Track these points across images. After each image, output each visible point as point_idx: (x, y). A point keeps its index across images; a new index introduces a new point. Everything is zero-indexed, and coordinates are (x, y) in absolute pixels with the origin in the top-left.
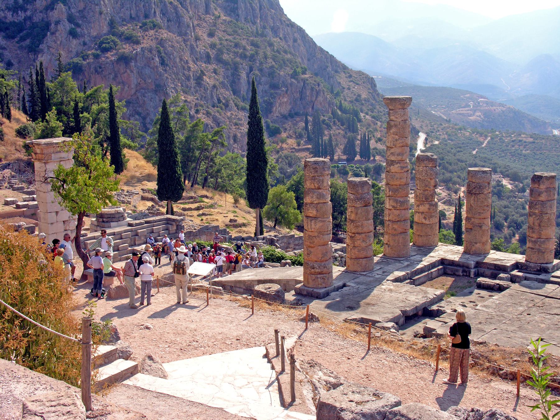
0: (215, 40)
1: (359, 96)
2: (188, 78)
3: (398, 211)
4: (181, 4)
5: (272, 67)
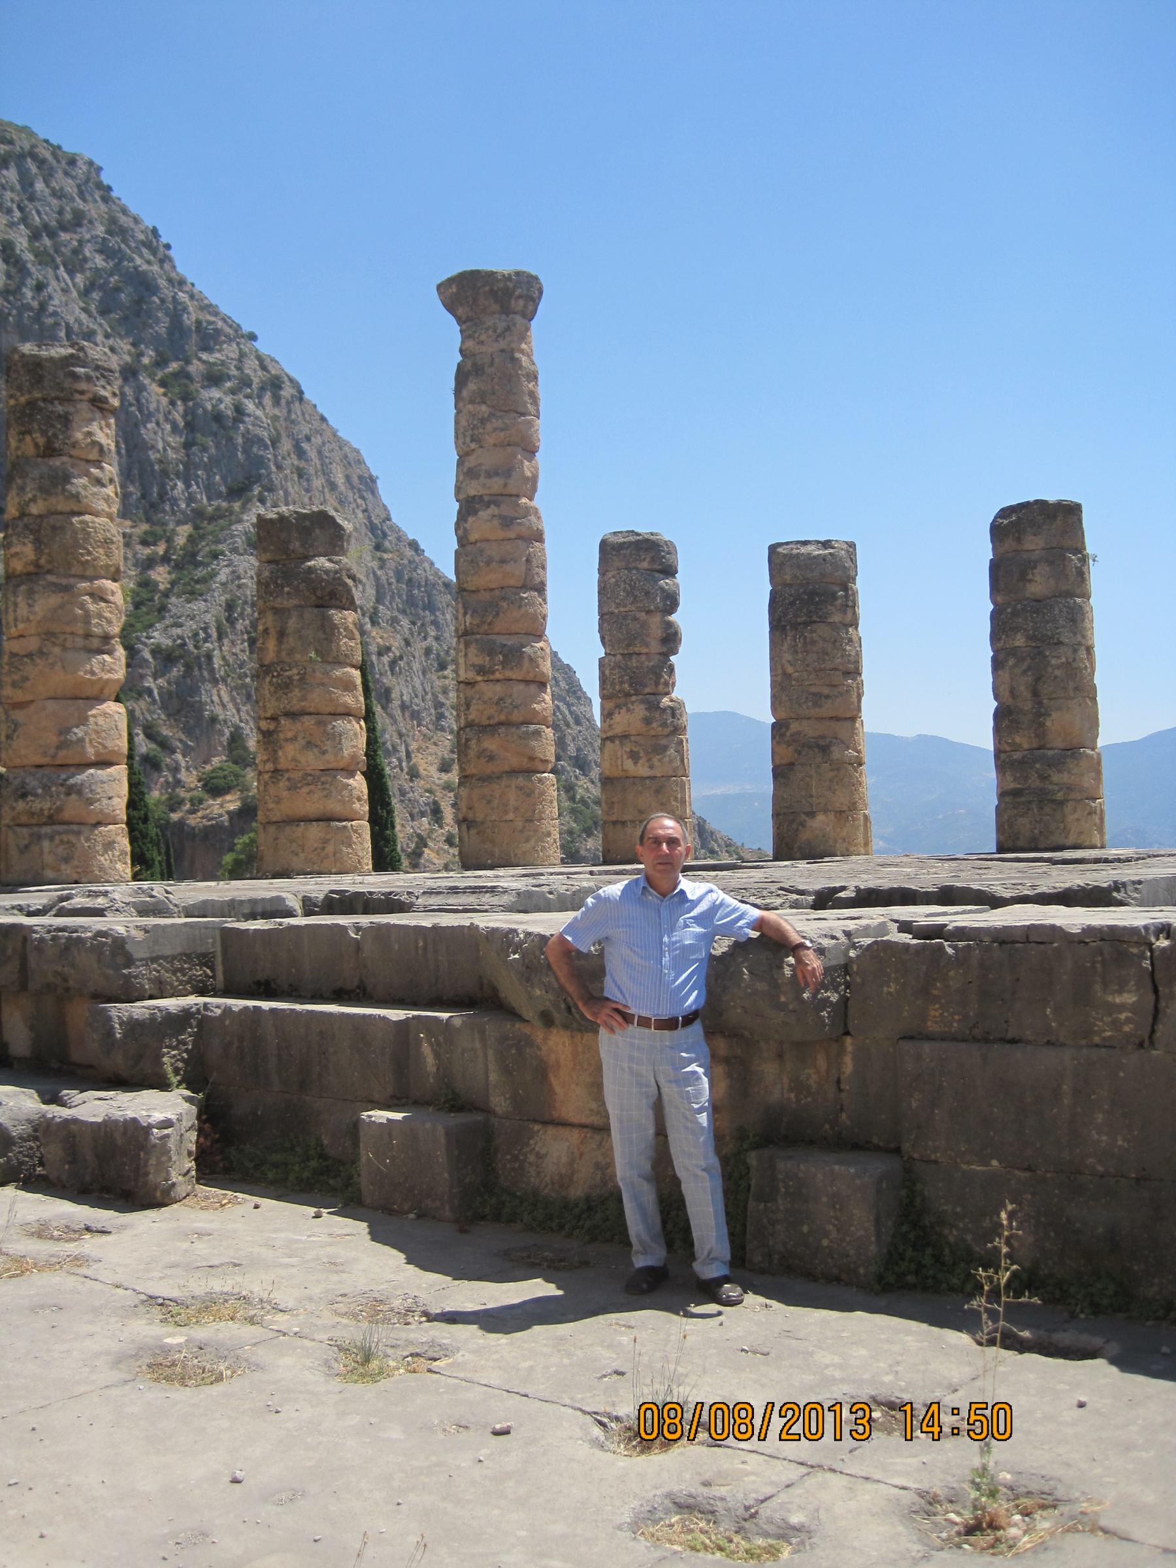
3: (498, 688)
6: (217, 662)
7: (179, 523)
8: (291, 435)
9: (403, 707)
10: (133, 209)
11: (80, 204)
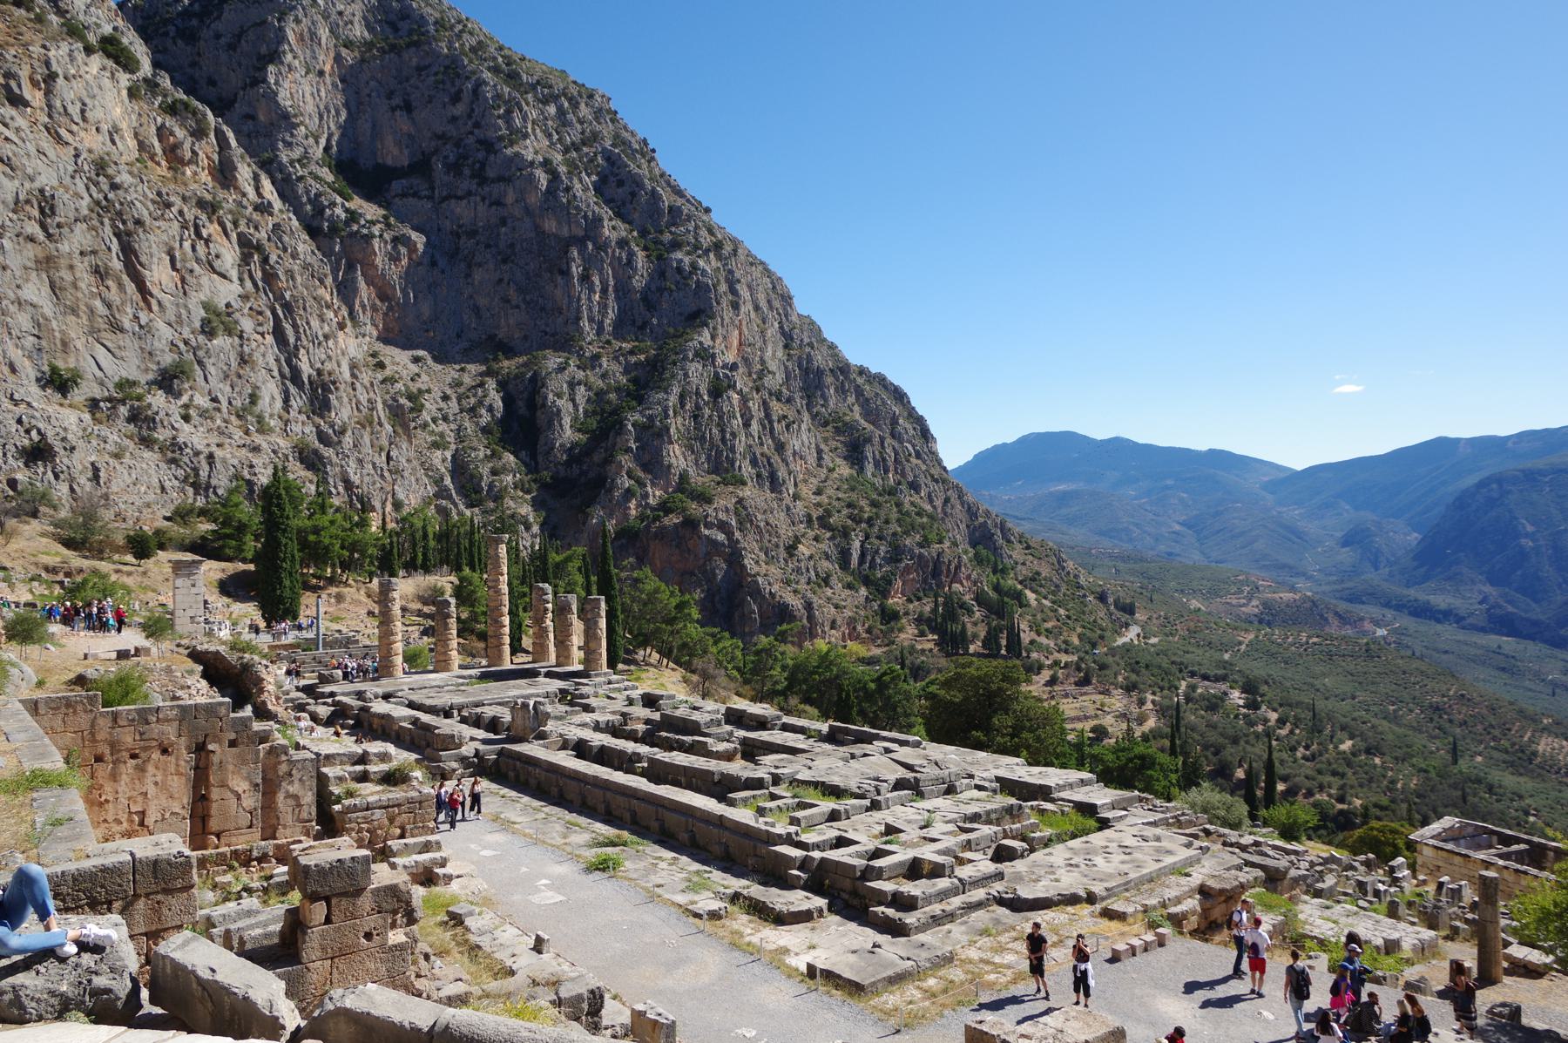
0: (824, 499)
1: (1038, 573)
2: (777, 546)
5: (894, 534)
6: (672, 431)
8: (727, 280)
9: (795, 453)
10: (631, 127)
11: (598, 128)
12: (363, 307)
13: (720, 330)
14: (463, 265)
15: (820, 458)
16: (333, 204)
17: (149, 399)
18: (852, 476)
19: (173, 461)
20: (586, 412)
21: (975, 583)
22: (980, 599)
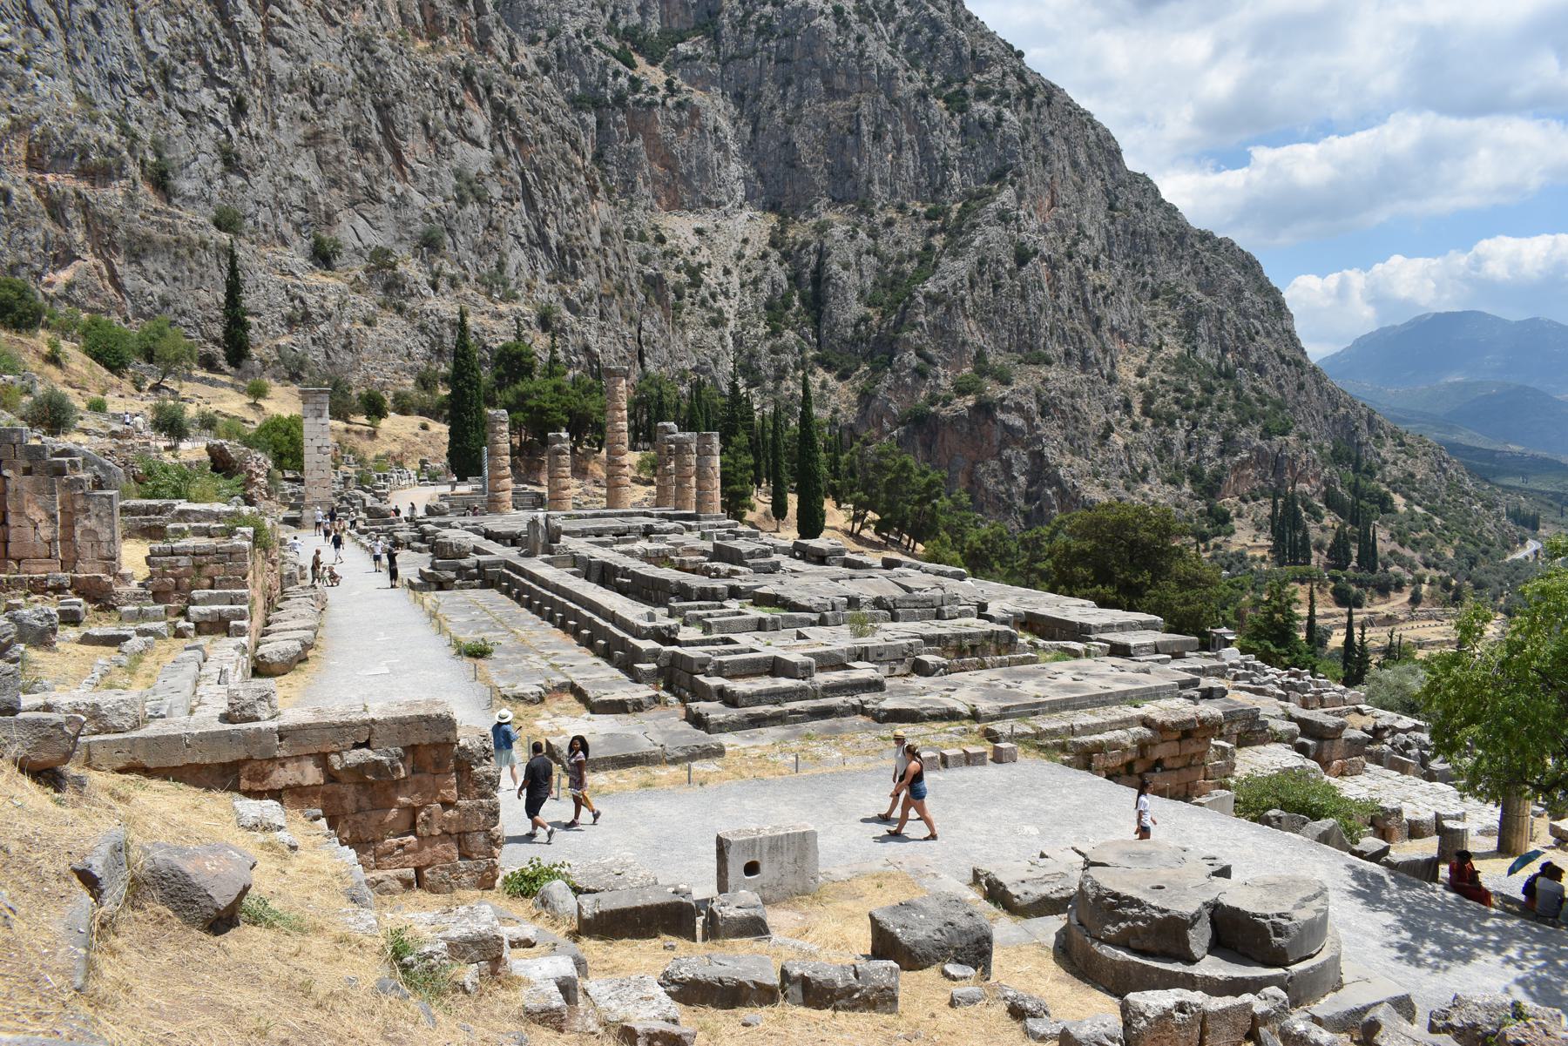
0: (1146, 381)
1: (1412, 475)
4: (1094, 332)
5: (1229, 423)
6: (968, 304)
7: (955, 202)
9: (1112, 330)
12: (645, 178)
13: (1028, 189)
14: (748, 130)
15: (1142, 336)
16: (617, 74)
17: (401, 268)
18: (1180, 355)
19: (422, 329)
20: (875, 284)
21: (1326, 483)
22: (1331, 501)
